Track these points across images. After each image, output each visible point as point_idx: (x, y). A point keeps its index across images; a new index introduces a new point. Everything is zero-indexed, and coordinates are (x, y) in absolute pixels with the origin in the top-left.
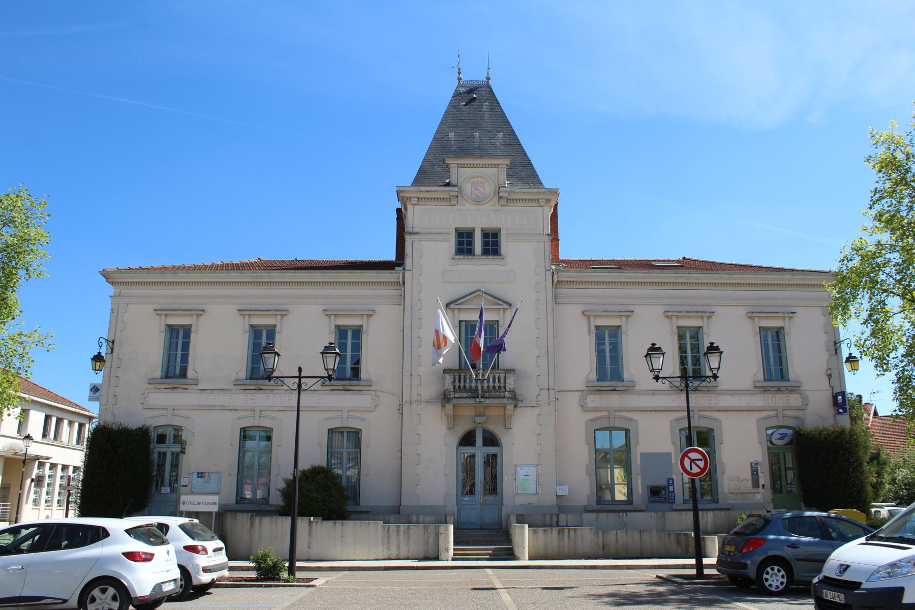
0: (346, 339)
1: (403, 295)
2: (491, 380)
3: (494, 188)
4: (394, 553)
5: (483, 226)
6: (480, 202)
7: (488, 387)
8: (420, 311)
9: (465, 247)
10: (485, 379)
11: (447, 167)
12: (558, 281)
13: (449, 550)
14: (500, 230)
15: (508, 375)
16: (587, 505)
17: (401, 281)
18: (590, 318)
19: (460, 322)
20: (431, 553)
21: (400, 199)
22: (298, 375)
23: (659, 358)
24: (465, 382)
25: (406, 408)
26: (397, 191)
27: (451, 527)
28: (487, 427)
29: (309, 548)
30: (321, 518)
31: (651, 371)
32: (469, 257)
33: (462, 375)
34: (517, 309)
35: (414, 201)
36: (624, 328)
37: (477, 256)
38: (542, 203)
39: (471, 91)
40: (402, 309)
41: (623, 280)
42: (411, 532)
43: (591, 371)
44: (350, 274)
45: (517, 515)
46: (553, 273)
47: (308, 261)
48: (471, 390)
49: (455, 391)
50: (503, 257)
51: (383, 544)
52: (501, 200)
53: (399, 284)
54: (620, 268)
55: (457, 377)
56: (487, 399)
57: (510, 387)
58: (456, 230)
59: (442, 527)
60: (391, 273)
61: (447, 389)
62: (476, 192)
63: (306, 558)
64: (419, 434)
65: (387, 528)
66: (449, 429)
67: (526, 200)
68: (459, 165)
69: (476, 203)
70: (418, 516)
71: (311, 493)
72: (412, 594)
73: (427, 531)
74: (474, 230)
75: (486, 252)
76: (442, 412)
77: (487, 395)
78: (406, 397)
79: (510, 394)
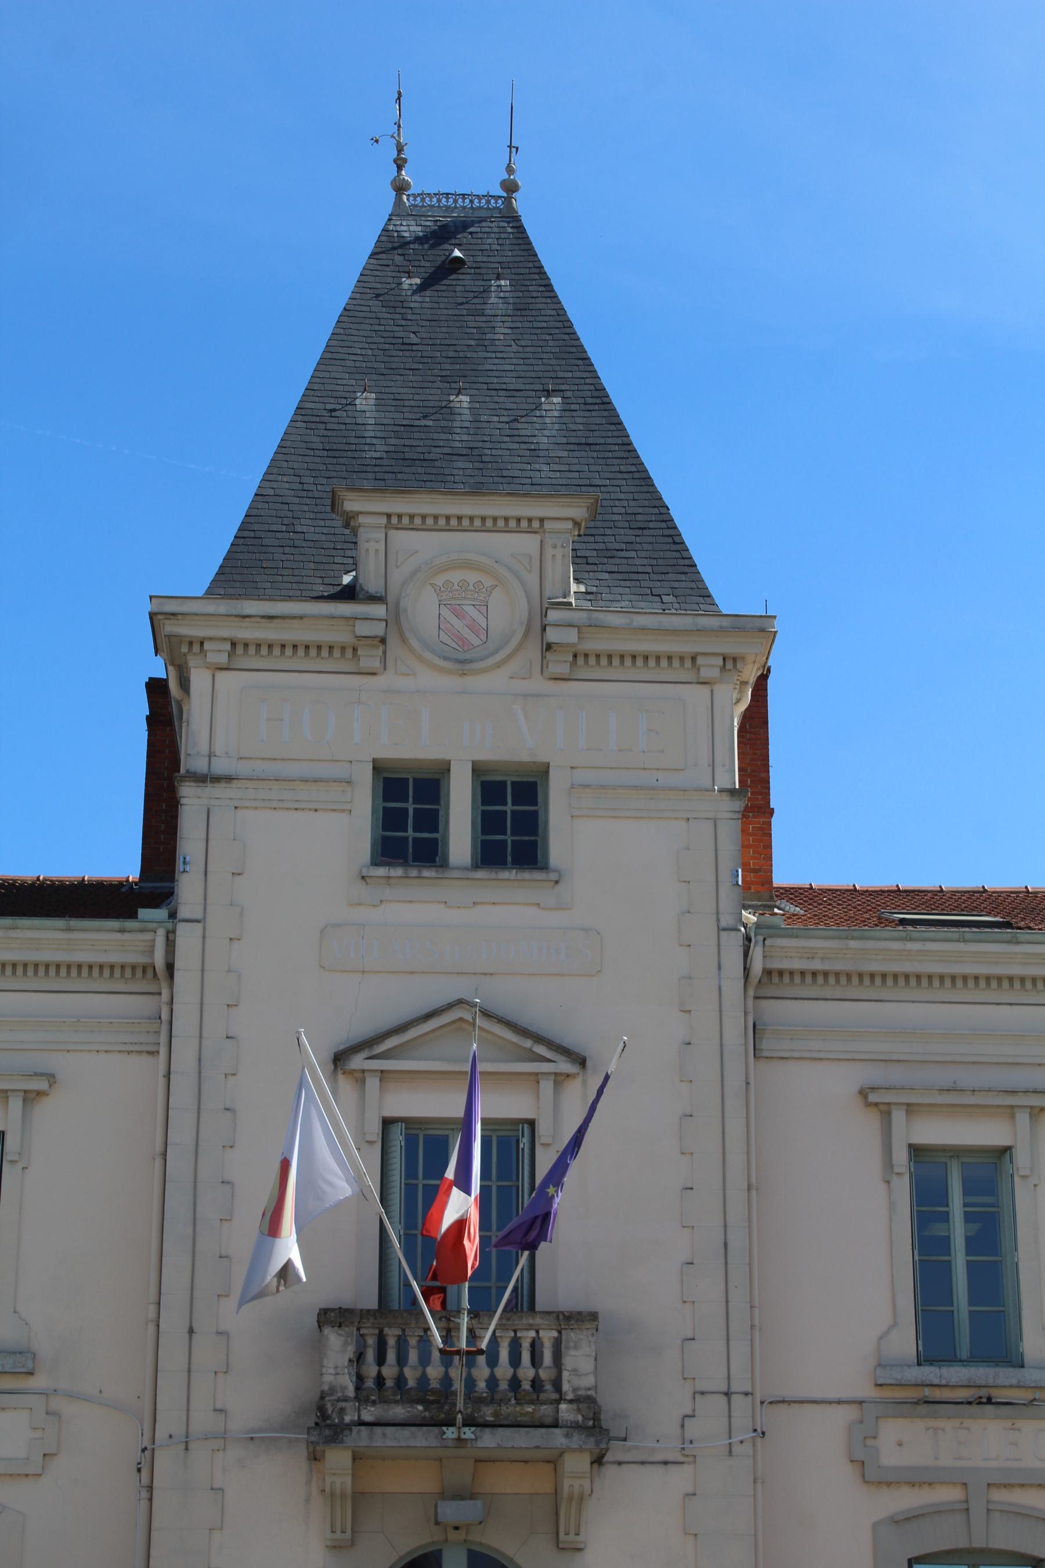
1: (165, 1016)
2: (504, 1354)
6: (471, 661)
7: (492, 1382)
8: (231, 1079)
9: (410, 833)
10: (481, 1352)
11: (347, 525)
15: (570, 1336)
17: (159, 959)
18: (889, 1113)
19: (387, 1123)
21: (163, 644)
24: (402, 1360)
25: (165, 1462)
26: (152, 616)
28: (484, 1541)
32: (426, 873)
33: (392, 1335)
34: (607, 1078)
37: (453, 869)
38: (710, 669)
41: (1017, 970)
43: (895, 1325)
46: (749, 940)
48: (423, 1393)
52: (549, 656)
54: (1008, 925)
56: (488, 1430)
58: (378, 768)
60: (122, 931)
61: (332, 1390)
62: (454, 621)
66: (335, 1547)
67: (646, 658)
68: (394, 520)
69: (458, 666)
74: (444, 769)
76: (309, 1481)
77: (488, 1413)
78: (169, 1422)
79: (579, 1410)
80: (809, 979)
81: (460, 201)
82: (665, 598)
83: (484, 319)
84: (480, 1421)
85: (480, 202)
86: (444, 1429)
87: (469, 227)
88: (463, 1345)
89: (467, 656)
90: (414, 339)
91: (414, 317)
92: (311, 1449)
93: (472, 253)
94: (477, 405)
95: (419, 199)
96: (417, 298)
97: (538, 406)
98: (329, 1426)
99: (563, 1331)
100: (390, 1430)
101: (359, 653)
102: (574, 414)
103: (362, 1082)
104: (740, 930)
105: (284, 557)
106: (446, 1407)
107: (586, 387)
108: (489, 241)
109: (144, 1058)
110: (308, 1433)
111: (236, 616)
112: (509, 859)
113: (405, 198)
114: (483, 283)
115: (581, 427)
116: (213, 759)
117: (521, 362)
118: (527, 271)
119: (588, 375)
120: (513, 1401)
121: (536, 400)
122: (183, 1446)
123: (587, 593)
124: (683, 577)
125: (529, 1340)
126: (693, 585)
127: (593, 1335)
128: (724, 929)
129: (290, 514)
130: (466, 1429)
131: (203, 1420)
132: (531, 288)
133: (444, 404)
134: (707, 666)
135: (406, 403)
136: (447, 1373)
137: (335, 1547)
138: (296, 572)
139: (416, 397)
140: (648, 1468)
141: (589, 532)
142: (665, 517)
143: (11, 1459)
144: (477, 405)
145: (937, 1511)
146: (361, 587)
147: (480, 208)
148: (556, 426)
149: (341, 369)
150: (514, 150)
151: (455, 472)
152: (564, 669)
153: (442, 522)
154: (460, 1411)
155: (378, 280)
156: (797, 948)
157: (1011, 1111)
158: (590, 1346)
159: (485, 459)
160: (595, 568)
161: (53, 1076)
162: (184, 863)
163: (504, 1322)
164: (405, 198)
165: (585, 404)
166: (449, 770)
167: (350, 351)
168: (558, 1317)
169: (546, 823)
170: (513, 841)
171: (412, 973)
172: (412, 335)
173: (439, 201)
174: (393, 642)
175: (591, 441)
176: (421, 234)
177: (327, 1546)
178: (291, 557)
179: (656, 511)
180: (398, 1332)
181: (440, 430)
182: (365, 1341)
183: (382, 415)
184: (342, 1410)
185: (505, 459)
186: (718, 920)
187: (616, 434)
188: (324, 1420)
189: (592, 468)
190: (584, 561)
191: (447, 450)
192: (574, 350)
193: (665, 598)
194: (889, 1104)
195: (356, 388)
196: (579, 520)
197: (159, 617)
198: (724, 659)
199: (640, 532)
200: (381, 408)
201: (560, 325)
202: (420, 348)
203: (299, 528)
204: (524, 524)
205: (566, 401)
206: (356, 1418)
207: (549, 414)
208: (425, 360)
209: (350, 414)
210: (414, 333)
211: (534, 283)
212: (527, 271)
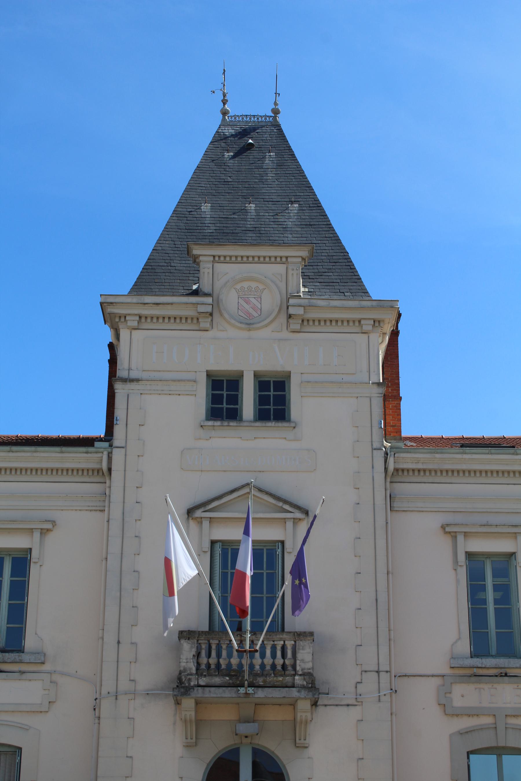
1: (107, 493)
2: (268, 652)
6: (253, 324)
7: (263, 666)
8: (138, 522)
9: (225, 405)
10: (256, 651)
11: (195, 261)
12: (396, 470)
14: (290, 376)
15: (301, 643)
18: (456, 537)
19: (213, 543)
21: (108, 319)
24: (219, 656)
25: (106, 706)
26: (101, 304)
28: (260, 743)
32: (232, 424)
33: (214, 643)
34: (315, 517)
35: (133, 322)
37: (245, 421)
38: (367, 326)
39: (244, 133)
40: (106, 519)
43: (459, 638)
44: (11, 454)
46: (387, 454)
48: (229, 672)
49: (199, 672)
52: (291, 321)
53: (101, 473)
55: (203, 646)
56: (260, 689)
57: (303, 666)
60: (87, 453)
61: (185, 670)
64: (131, 757)
66: (188, 746)
68: (217, 258)
69: (247, 326)
74: (241, 375)
76: (175, 715)
77: (260, 681)
78: (108, 686)
79: (304, 679)
80: (416, 473)
81: (252, 118)
82: (346, 294)
83: (263, 170)
84: (257, 684)
85: (262, 119)
86: (239, 688)
87: (256, 130)
88: (247, 647)
89: (251, 322)
90: (230, 179)
91: (230, 170)
92: (175, 699)
93: (258, 141)
94: (259, 208)
95: (233, 118)
96: (231, 161)
97: (287, 208)
98: (183, 687)
99: (297, 641)
100: (213, 689)
101: (200, 320)
102: (304, 211)
103: (201, 523)
104: (383, 450)
105: (165, 278)
106: (240, 678)
107: (310, 200)
108: (266, 136)
109: (98, 513)
110: (173, 690)
111: (141, 303)
112: (272, 417)
113: (227, 117)
114: (262, 154)
115: (307, 217)
116: (130, 371)
117: (280, 189)
118: (283, 148)
119: (311, 194)
120: (273, 675)
121: (286, 206)
122: (114, 697)
123: (309, 292)
124: (355, 284)
125: (281, 646)
126: (360, 288)
127: (311, 643)
128: (375, 449)
129: (169, 258)
130: (250, 689)
131: (124, 685)
132: (285, 156)
133: (243, 208)
134: (366, 324)
135: (225, 208)
136: (240, 662)
137: (187, 746)
138: (171, 284)
139: (230, 205)
140: (340, 708)
141: (310, 264)
142: (346, 257)
143: (33, 704)
144: (259, 208)
146: (201, 290)
147: (262, 121)
148: (296, 217)
149: (195, 193)
150: (278, 95)
151: (247, 238)
152: (297, 327)
153: (239, 259)
154: (246, 680)
155: (213, 154)
156: (411, 458)
158: (310, 648)
159: (262, 232)
160: (313, 280)
161: (54, 522)
162: (117, 420)
163: (268, 637)
164: (227, 117)
165: (310, 207)
166: (243, 376)
167: (199, 185)
168: (294, 634)
169: (290, 400)
170: (273, 409)
171: (225, 471)
172: (229, 178)
173: (243, 119)
174: (216, 315)
175: (312, 223)
176: (234, 133)
177: (184, 746)
178: (169, 278)
179: (342, 254)
180: (217, 642)
181: (240, 219)
182: (201, 646)
183: (214, 213)
184: (190, 680)
185: (271, 232)
186: (372, 445)
187: (324, 220)
188: (181, 684)
189: (312, 236)
190: (308, 277)
191: (244, 229)
192: (305, 183)
193: (346, 294)
194: (456, 532)
195: (202, 202)
196: (304, 257)
197: (105, 304)
198: (374, 322)
199: (335, 264)
200: (213, 210)
201: (298, 172)
202: (232, 183)
203: (173, 264)
204: (278, 259)
205: (300, 206)
206: (196, 683)
207: (292, 212)
208: (235, 189)
209: (198, 213)
210: (229, 177)
211: (286, 154)
212: (283, 148)
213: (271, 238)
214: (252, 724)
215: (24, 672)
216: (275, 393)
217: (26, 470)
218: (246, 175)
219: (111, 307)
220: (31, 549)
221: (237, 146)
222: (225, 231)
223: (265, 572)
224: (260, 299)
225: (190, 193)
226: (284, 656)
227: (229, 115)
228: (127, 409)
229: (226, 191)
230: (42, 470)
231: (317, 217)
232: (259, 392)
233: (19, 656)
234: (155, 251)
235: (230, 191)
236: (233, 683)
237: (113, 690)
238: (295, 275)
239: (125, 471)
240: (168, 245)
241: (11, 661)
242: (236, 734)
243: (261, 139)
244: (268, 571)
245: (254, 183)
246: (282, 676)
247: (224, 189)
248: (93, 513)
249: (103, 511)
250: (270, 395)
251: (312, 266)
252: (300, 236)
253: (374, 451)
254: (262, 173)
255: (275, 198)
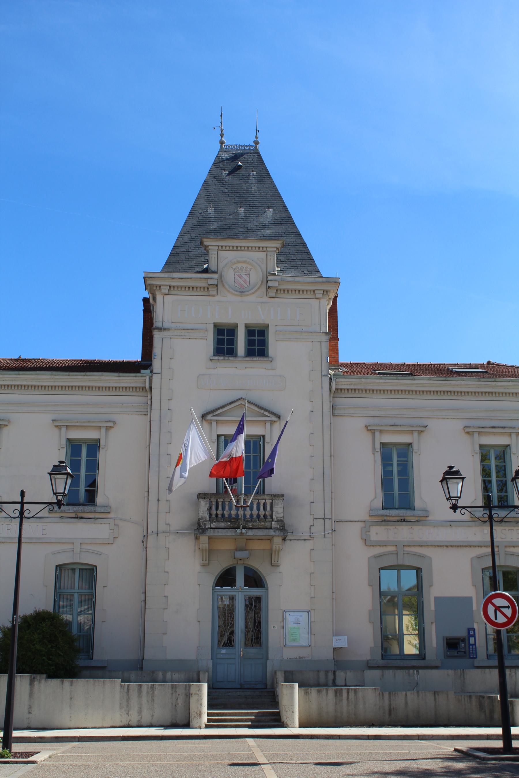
0: (80, 456)
1: (149, 403)
3: (261, 273)
4: (134, 718)
5: (247, 322)
6: (244, 292)
7: (251, 515)
9: (225, 346)
10: (248, 506)
11: (205, 249)
13: (202, 715)
14: (268, 327)
15: (275, 501)
16: (370, 660)
17: (147, 385)
18: (374, 433)
19: (218, 436)
20: (180, 719)
21: (148, 287)
22: (20, 500)
23: (458, 483)
24: (223, 509)
25: (151, 540)
26: (144, 278)
27: (205, 686)
28: (249, 563)
29: (30, 713)
30: (45, 676)
31: (448, 499)
32: (230, 358)
33: (220, 501)
34: (287, 422)
35: (165, 290)
36: (415, 446)
37: (239, 357)
38: (319, 294)
39: (235, 158)
40: (149, 420)
42: (156, 692)
43: (376, 498)
44: (86, 377)
45: (285, 672)
46: (331, 379)
47: (35, 360)
48: (230, 519)
49: (211, 520)
50: (270, 359)
51: (121, 708)
52: (269, 290)
54: (412, 374)
56: (250, 530)
57: (277, 515)
58: (215, 325)
59: (194, 686)
60: (136, 377)
61: (202, 518)
63: (26, 726)
64: (167, 572)
65: (126, 687)
66: (203, 565)
67: (299, 291)
68: (220, 248)
70: (165, 672)
71: (34, 645)
72: (156, 771)
73: (176, 692)
74: (236, 326)
75: (250, 353)
77: (250, 525)
78: (152, 528)
79: (278, 524)
80: (350, 391)
81: (241, 147)
82: (305, 272)
83: (248, 184)
84: (248, 527)
85: (247, 148)
86: (237, 530)
87: (243, 155)
88: (242, 504)
89: (243, 290)
90: (226, 191)
91: (226, 184)
92: (196, 536)
93: (245, 163)
94: (246, 211)
95: (228, 146)
96: (227, 178)
99: (273, 500)
100: (220, 530)
101: (209, 289)
102: (277, 214)
104: (328, 376)
105: (186, 259)
106: (237, 523)
107: (280, 206)
108: (250, 160)
109: (143, 416)
110: (195, 531)
111: (171, 278)
112: (256, 354)
113: (223, 146)
114: (248, 173)
115: (279, 218)
116: (164, 323)
117: (260, 198)
118: (262, 169)
119: (281, 202)
120: (258, 521)
121: (265, 210)
122: (156, 535)
123: (281, 270)
124: (311, 265)
125: (263, 503)
126: (314, 268)
127: (282, 501)
128: (324, 376)
129: (188, 246)
130: (243, 530)
131: (162, 527)
132: (263, 175)
133: (236, 211)
134: (318, 293)
135: (224, 211)
136: (237, 513)
137: (203, 565)
138: (189, 264)
139: (227, 209)
141: (281, 251)
142: (305, 247)
143: (104, 539)
144: (246, 211)
145: (388, 554)
146: (210, 269)
147: (247, 149)
148: (271, 218)
149: (203, 200)
150: (258, 131)
151: (239, 232)
152: (273, 294)
153: (235, 248)
154: (241, 524)
155: (215, 172)
156: (346, 381)
157: (412, 432)
158: (282, 504)
159: (249, 228)
160: (283, 263)
162: (155, 355)
163: (255, 497)
164: (223, 146)
165: (280, 211)
166: (237, 326)
167: (206, 194)
168: (272, 496)
169: (268, 342)
170: (257, 348)
171: (226, 390)
172: (226, 189)
173: (234, 147)
174: (220, 286)
175: (282, 223)
176: (228, 158)
177: (201, 565)
178: (188, 259)
179: (302, 245)
180: (222, 500)
181: (234, 219)
182: (212, 503)
183: (216, 214)
184: (205, 524)
185: (255, 228)
186: (322, 373)
187: (290, 220)
188: (200, 527)
189: (282, 231)
190: (280, 260)
191: (237, 226)
192: (276, 194)
193: (305, 272)
194: (374, 430)
195: (208, 206)
196: (278, 248)
197: (147, 278)
198: (324, 291)
199: (297, 251)
200: (216, 212)
201: (272, 186)
202: (228, 193)
203: (190, 250)
204: (261, 249)
205: (274, 210)
206: (209, 526)
207: (269, 214)
208: (230, 197)
209: (206, 214)
210: (226, 189)
211: (264, 173)
212: (262, 169)
213: (255, 233)
214: (244, 552)
215: (97, 519)
216: (258, 338)
217: (96, 387)
218: (237, 188)
219: (151, 280)
220: (99, 439)
221: (231, 167)
222: (224, 227)
223: (252, 455)
224: (248, 275)
225: (200, 200)
226: (265, 509)
227: (225, 144)
228: (162, 348)
229: (224, 199)
230: (106, 387)
231: (285, 218)
232: (248, 337)
233: (94, 508)
234: (178, 241)
235: (227, 199)
236: (233, 526)
237: (155, 530)
238: (272, 260)
239: (161, 389)
240: (186, 237)
241: (89, 511)
242: (235, 558)
243: (247, 162)
244: (254, 455)
245: (242, 193)
246: (264, 522)
247: (223, 197)
248: (140, 416)
249: (146, 415)
250: (255, 339)
251: (283, 252)
252: (274, 231)
253: (323, 377)
254: (248, 186)
255: (257, 204)
